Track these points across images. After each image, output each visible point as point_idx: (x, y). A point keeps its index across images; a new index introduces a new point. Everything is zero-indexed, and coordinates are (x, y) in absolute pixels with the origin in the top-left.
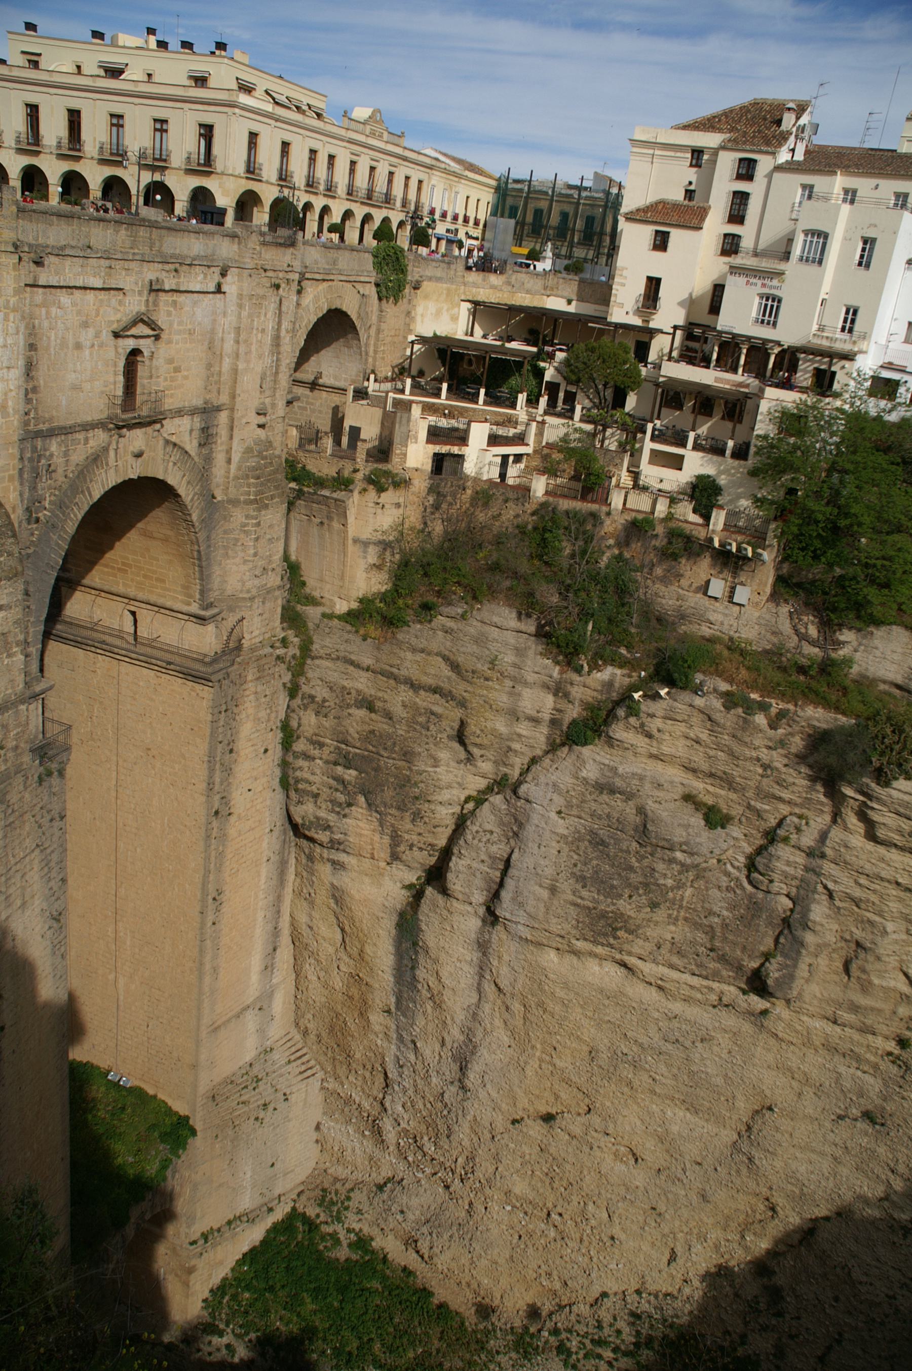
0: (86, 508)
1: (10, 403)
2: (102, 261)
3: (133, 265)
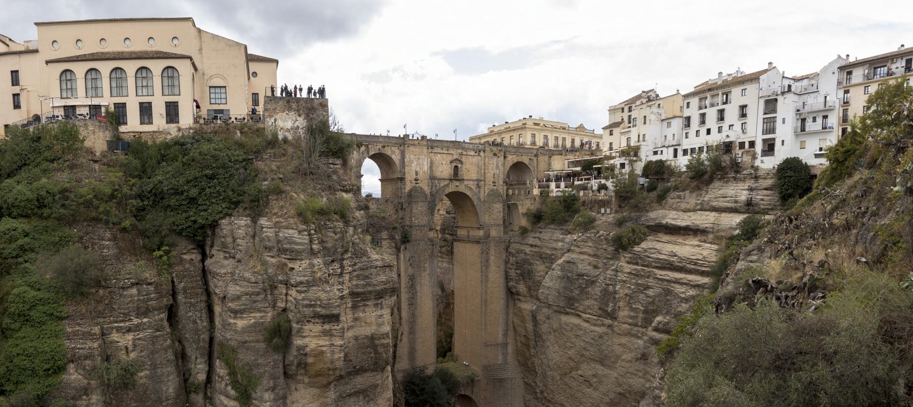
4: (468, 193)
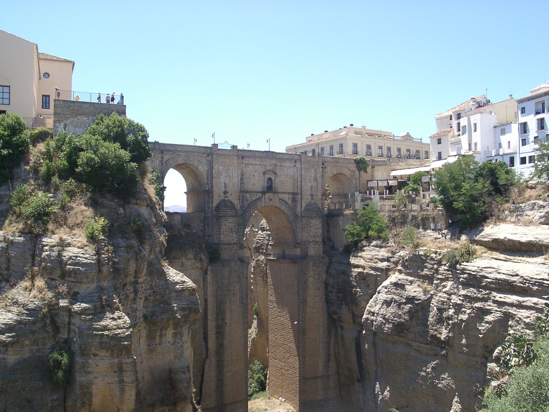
3: (268, 160)
4: (283, 208)
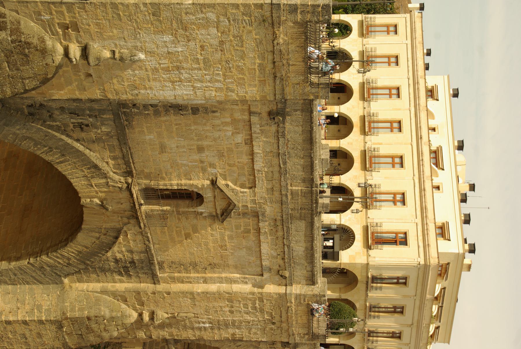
0: (48, 158)
1: (142, 91)
2: (277, 169)
3: (277, 194)
